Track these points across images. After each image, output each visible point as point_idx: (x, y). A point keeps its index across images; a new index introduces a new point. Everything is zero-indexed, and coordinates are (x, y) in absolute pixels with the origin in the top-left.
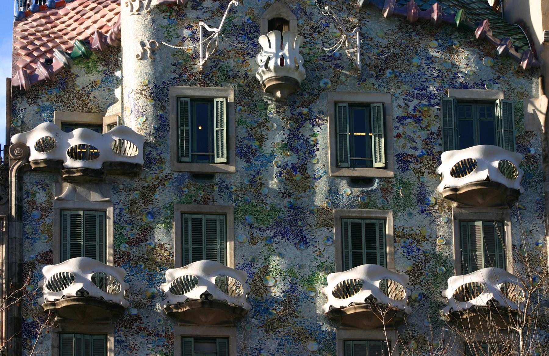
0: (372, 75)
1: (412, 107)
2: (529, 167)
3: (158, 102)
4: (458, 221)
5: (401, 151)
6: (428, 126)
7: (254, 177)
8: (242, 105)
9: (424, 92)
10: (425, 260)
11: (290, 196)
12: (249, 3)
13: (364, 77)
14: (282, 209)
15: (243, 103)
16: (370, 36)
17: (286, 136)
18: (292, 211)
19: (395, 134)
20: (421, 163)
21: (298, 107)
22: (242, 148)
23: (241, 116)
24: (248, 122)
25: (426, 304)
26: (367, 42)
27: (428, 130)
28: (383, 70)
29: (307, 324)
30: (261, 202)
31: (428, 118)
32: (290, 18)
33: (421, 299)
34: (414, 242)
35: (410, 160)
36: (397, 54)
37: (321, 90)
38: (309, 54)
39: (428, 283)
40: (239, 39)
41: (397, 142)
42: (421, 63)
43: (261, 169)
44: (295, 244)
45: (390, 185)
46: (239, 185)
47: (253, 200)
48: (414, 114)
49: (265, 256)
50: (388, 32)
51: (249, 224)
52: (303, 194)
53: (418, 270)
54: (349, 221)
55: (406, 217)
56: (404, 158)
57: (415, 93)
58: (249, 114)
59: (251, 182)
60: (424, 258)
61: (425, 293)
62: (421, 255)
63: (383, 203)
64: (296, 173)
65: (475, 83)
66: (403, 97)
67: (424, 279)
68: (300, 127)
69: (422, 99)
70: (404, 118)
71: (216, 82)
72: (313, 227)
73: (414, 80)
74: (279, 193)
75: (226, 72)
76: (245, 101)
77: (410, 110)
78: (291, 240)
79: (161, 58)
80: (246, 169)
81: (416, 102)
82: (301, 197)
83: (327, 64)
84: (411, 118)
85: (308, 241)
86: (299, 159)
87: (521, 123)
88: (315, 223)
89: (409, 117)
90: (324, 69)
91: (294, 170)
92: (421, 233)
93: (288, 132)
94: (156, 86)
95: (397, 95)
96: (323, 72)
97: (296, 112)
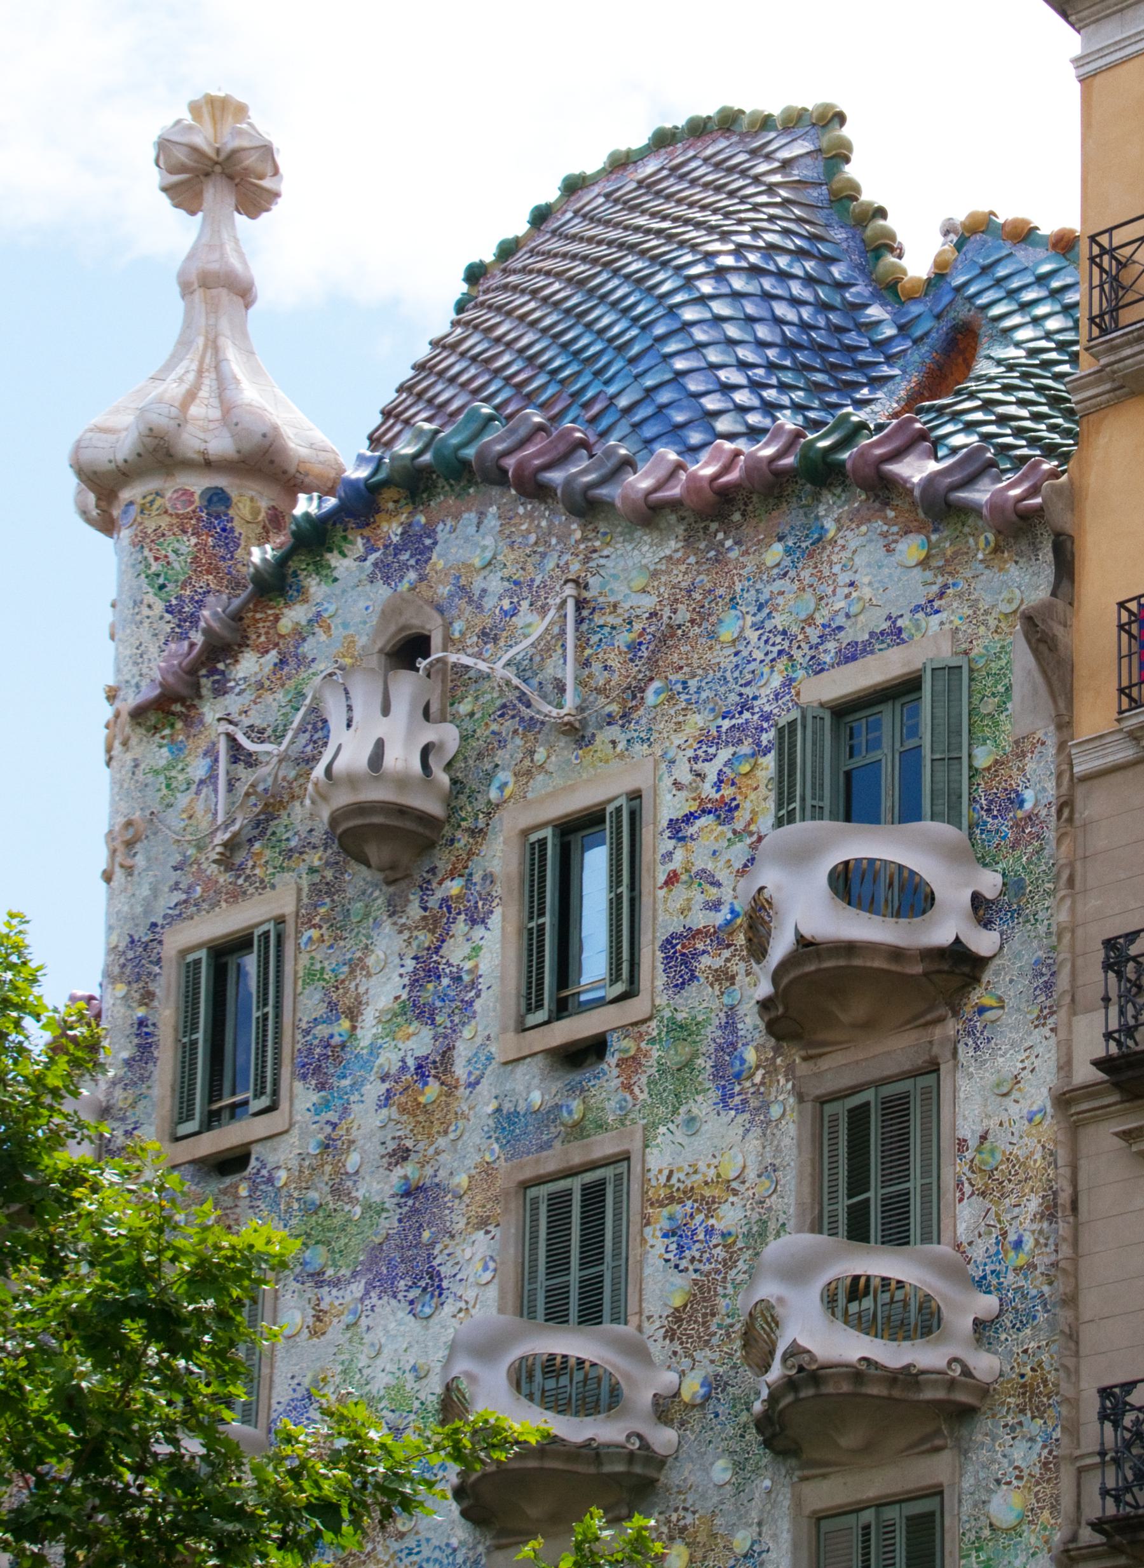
0: (609, 715)
1: (712, 777)
2: (1020, 858)
3: (135, 986)
4: (809, 1106)
5: (675, 925)
6: (752, 821)
7: (335, 1126)
8: (314, 926)
9: (747, 715)
10: (724, 1260)
11: (405, 1159)
12: (345, 625)
13: (590, 730)
14: (387, 1206)
15: (317, 920)
16: (612, 600)
17: (406, 981)
18: (410, 1203)
19: (662, 878)
20: (728, 946)
21: (440, 883)
22: (310, 1051)
23: (312, 958)
24: (328, 968)
25: (720, 1410)
26: (601, 622)
27: (751, 834)
28: (636, 691)
29: (426, 1552)
30: (346, 1199)
31: (752, 796)
32: (428, 627)
33: (707, 1397)
34: (699, 1211)
35: (700, 946)
36: (679, 627)
37: (492, 809)
38: (472, 714)
39: (728, 1335)
40: (316, 737)
41: (666, 900)
42: (742, 630)
43: (352, 1099)
44: (412, 1302)
45: (643, 1045)
46: (294, 1163)
47: (329, 1198)
48: (718, 796)
49: (342, 1363)
50: (658, 567)
51: (311, 1275)
52: (442, 1142)
53: (705, 1300)
54: (544, 1191)
55: (679, 1136)
56: (684, 947)
57: (724, 729)
58: (331, 947)
59: (327, 1146)
60: (723, 1255)
61: (721, 1370)
62: (716, 1246)
63: (621, 1108)
64: (426, 1084)
65: (872, 634)
66: (690, 753)
67: (720, 1327)
68: (443, 941)
69: (740, 741)
70: (689, 818)
71: (262, 881)
72: (458, 1239)
73: (723, 690)
74: (383, 1157)
75: (283, 845)
76: (322, 910)
77: (707, 789)
78: (400, 1296)
79: (148, 859)
80: (318, 1109)
81: (725, 754)
82: (437, 1153)
83: (509, 724)
84: (710, 812)
85: (445, 1284)
86: (435, 1038)
87: (1002, 717)
88: (461, 1225)
89: (703, 811)
90: (502, 743)
91: (423, 1075)
92: (719, 1176)
93: (410, 964)
94: (132, 942)
95: (671, 755)
96: (501, 757)
97: (433, 902)
